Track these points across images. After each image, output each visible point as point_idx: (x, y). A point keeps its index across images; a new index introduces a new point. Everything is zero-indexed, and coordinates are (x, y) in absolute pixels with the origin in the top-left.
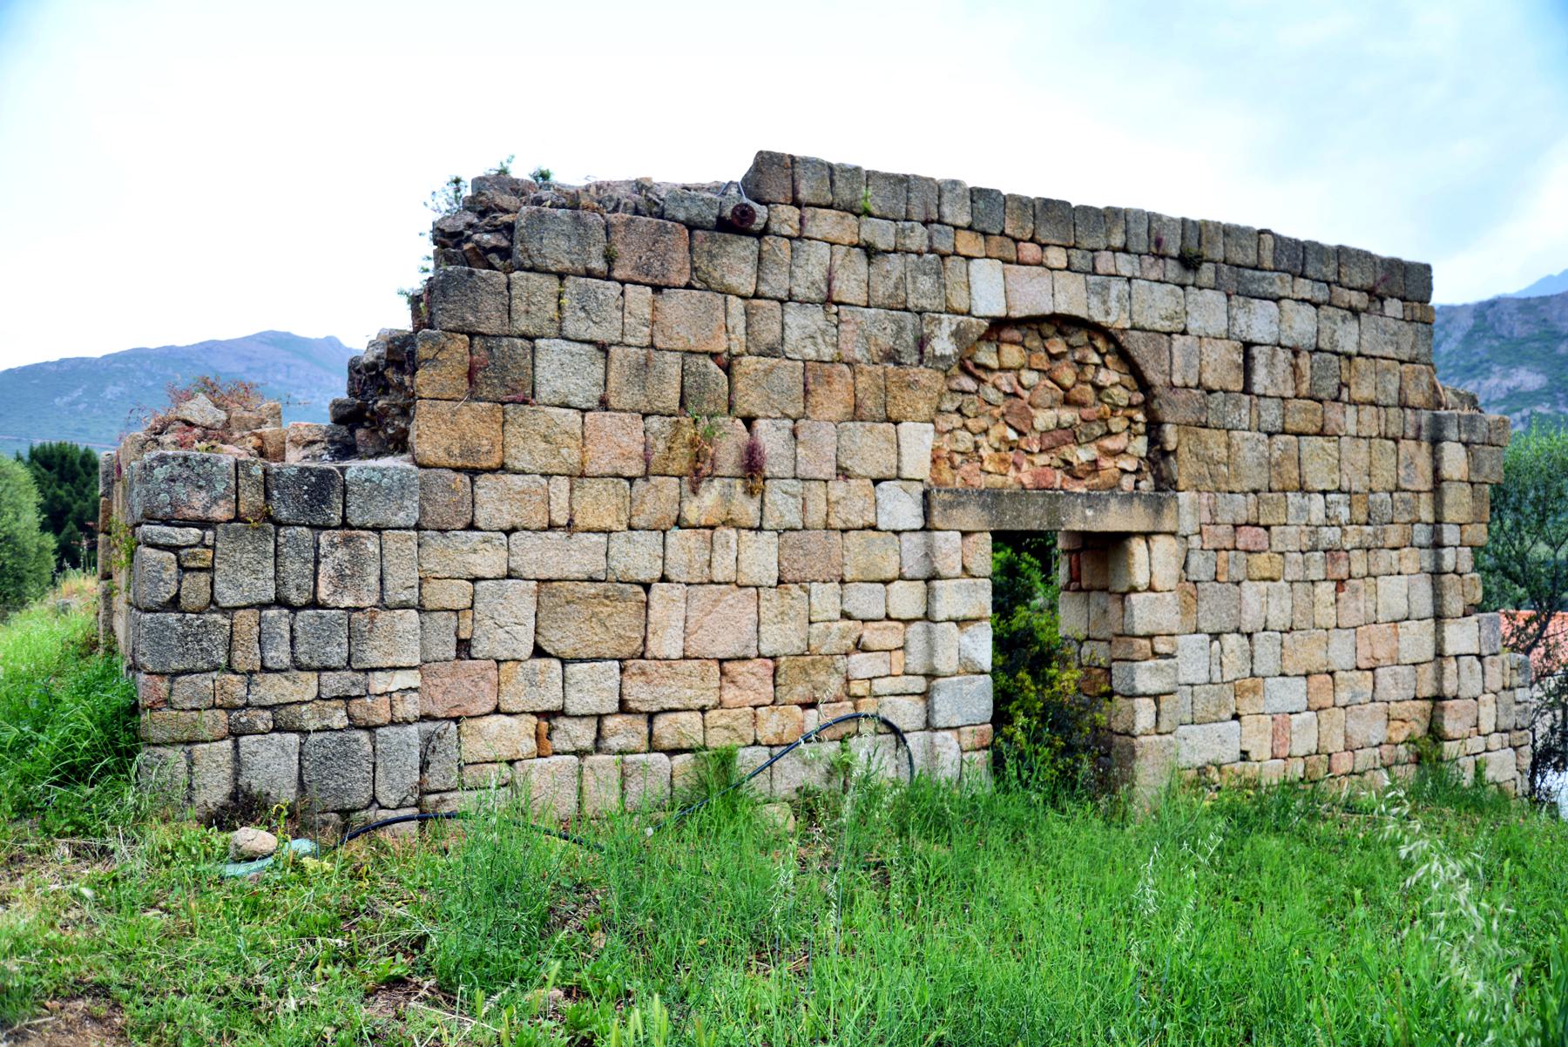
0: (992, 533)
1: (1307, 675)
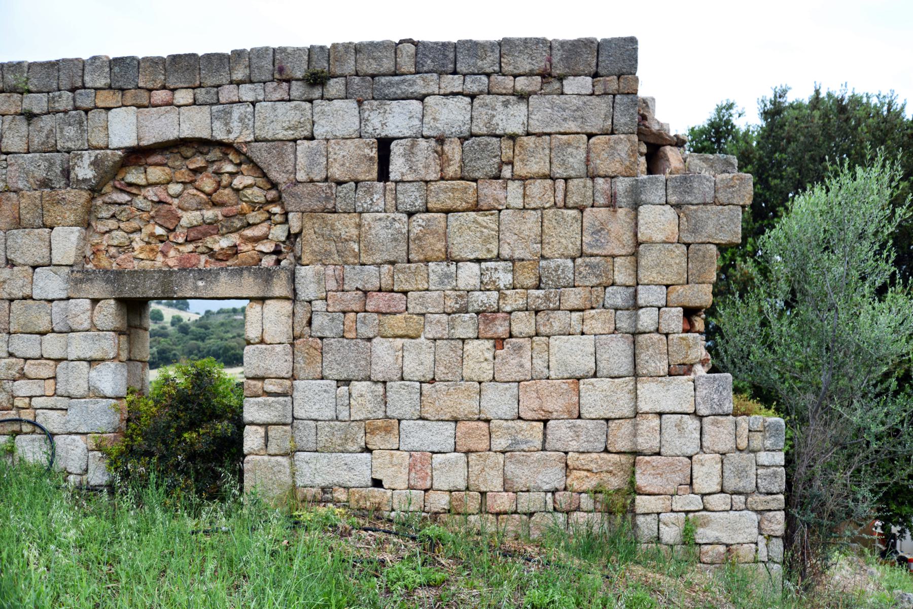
0: (115, 299)
1: (456, 421)
